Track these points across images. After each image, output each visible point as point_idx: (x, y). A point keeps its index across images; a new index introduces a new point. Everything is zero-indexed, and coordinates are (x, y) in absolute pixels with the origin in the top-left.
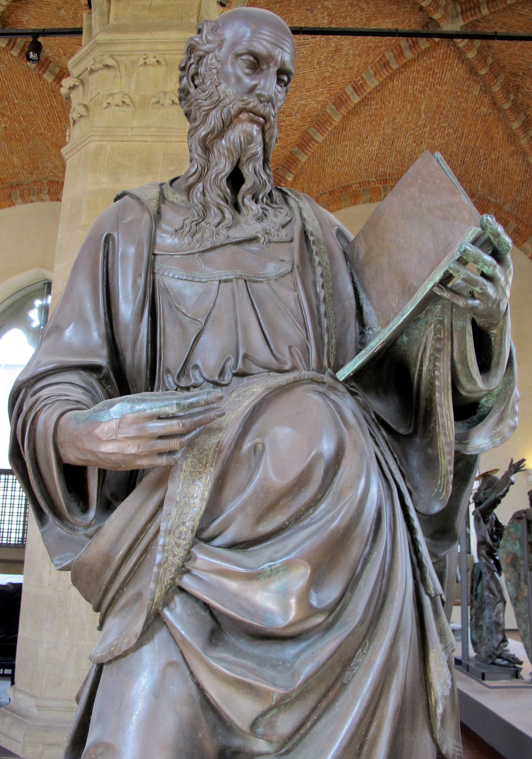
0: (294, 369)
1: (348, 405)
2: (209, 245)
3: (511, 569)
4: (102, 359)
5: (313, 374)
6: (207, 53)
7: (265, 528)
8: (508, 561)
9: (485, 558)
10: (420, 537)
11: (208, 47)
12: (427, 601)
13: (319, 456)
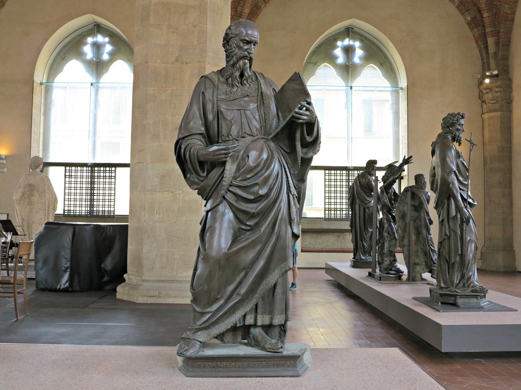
0: (257, 135)
1: (272, 144)
2: (234, 98)
3: (401, 221)
4: (204, 132)
5: (262, 137)
6: (232, 37)
7: (248, 176)
8: (400, 216)
9: (386, 214)
10: (290, 179)
11: (232, 36)
12: (290, 195)
13: (263, 159)
